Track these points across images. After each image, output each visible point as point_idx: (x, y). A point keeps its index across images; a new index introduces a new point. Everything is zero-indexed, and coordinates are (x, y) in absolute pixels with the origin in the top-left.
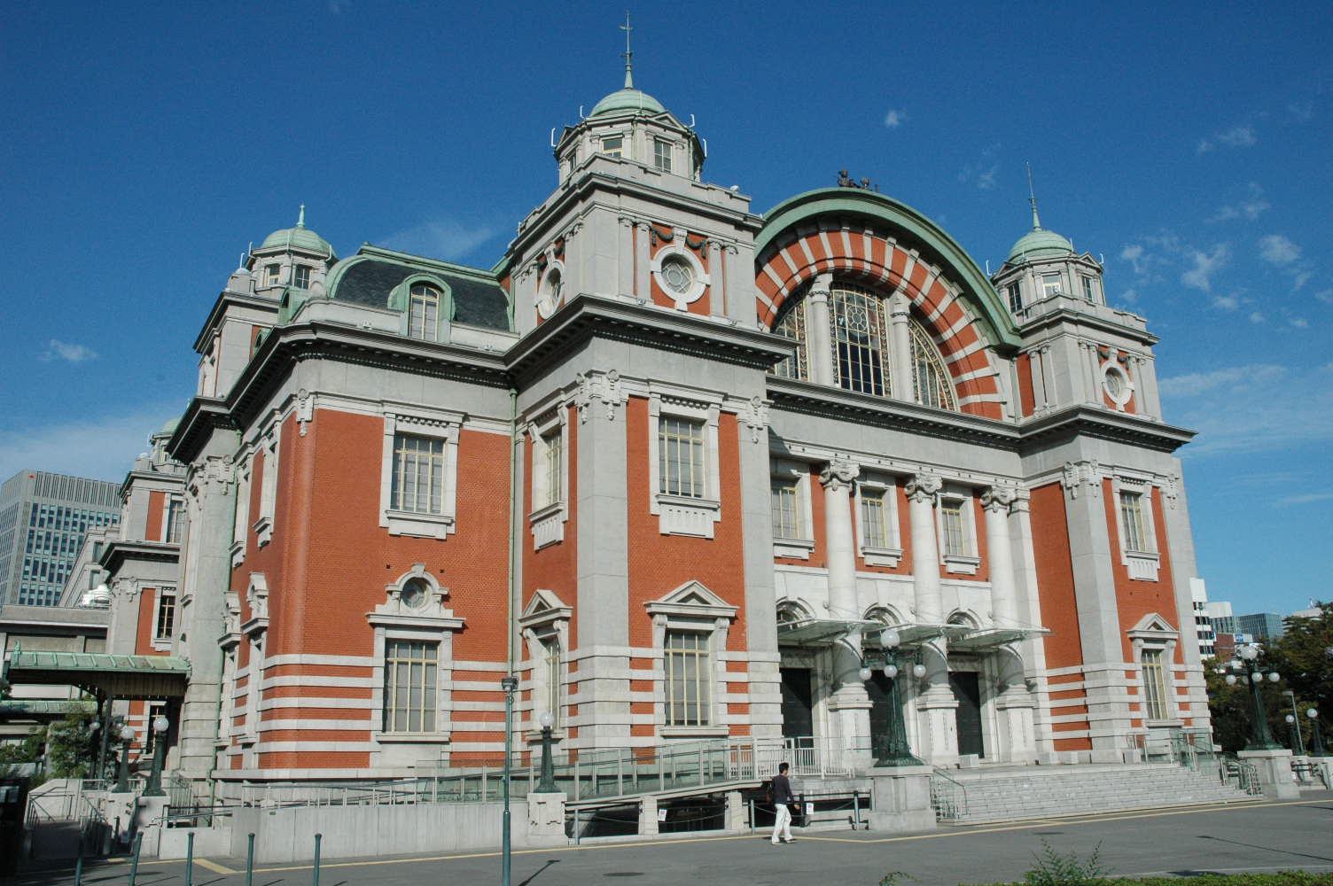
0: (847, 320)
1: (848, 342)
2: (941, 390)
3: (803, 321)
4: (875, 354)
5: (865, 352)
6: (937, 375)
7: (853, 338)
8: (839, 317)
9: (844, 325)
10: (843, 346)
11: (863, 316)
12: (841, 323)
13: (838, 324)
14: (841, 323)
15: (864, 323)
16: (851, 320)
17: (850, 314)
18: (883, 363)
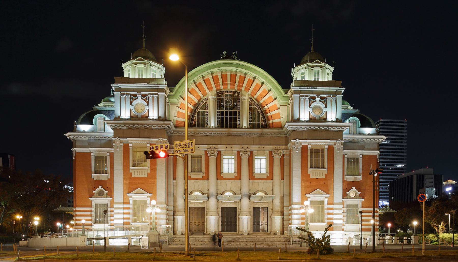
0: (225, 103)
1: (224, 111)
2: (262, 120)
3: (208, 107)
4: (235, 113)
5: (231, 113)
6: (261, 115)
7: (226, 108)
8: (221, 103)
9: (223, 105)
10: (222, 113)
11: (231, 101)
12: (222, 105)
13: (221, 105)
14: (222, 105)
15: (231, 103)
16: (226, 103)
17: (226, 101)
18: (238, 115)
